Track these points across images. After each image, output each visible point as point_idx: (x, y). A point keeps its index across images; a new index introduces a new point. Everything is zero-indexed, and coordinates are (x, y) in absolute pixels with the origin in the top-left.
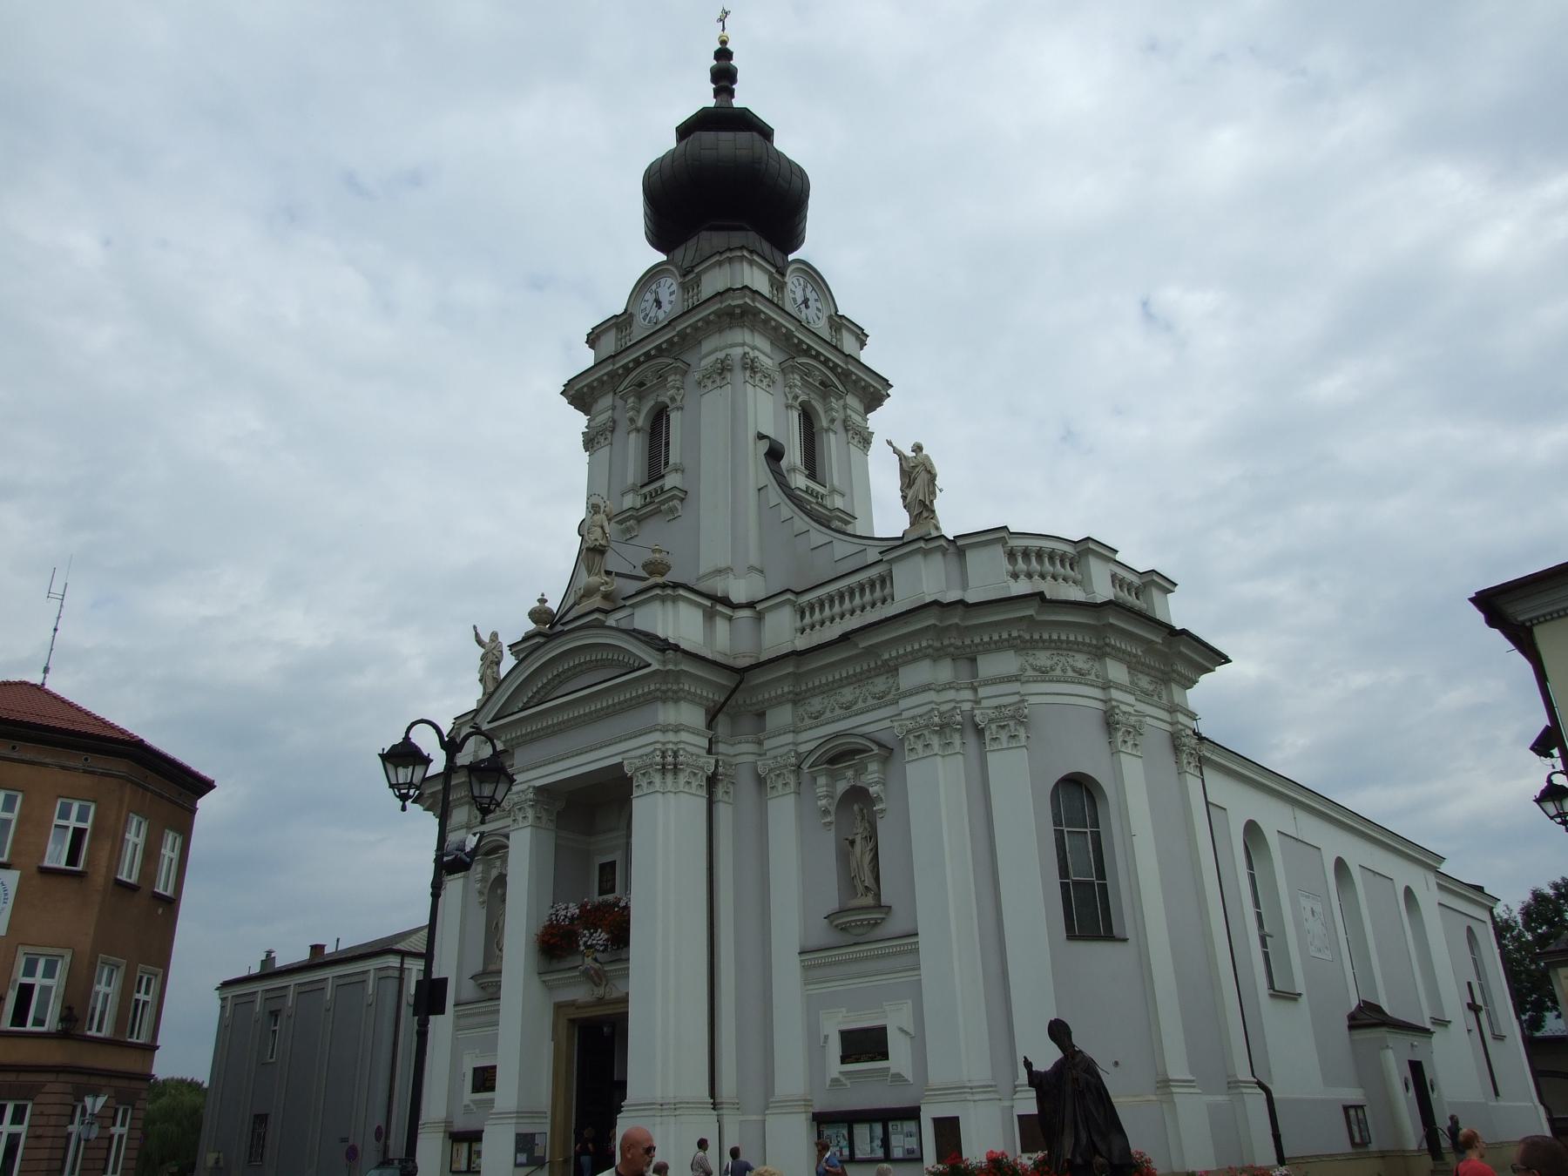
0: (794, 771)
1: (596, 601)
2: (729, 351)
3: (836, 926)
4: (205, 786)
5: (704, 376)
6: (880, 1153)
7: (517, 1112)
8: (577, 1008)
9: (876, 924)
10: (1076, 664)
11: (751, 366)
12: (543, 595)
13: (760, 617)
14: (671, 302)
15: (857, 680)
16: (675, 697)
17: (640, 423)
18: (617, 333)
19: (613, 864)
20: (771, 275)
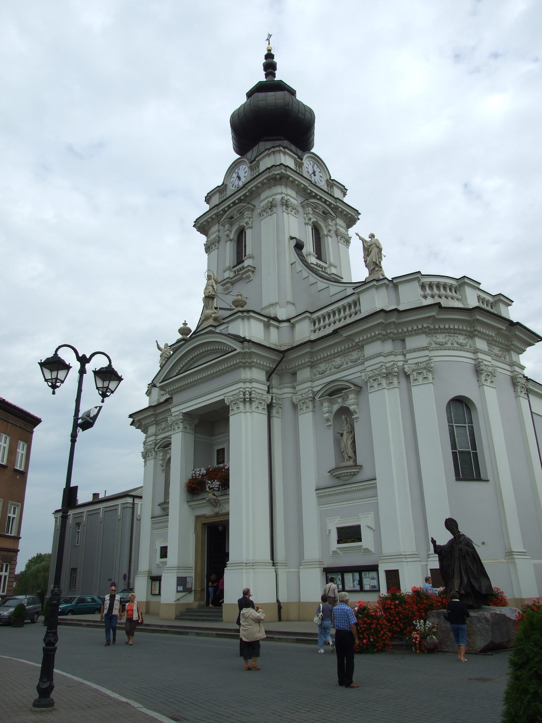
0: (311, 400)
1: (211, 322)
2: (274, 197)
3: (334, 476)
4: (36, 421)
5: (262, 211)
6: (358, 588)
7: (177, 567)
8: (206, 518)
10: (458, 341)
11: (286, 204)
12: (185, 321)
13: (293, 326)
14: (245, 177)
16: (250, 365)
17: (232, 236)
18: (219, 195)
19: (223, 450)
20: (295, 159)
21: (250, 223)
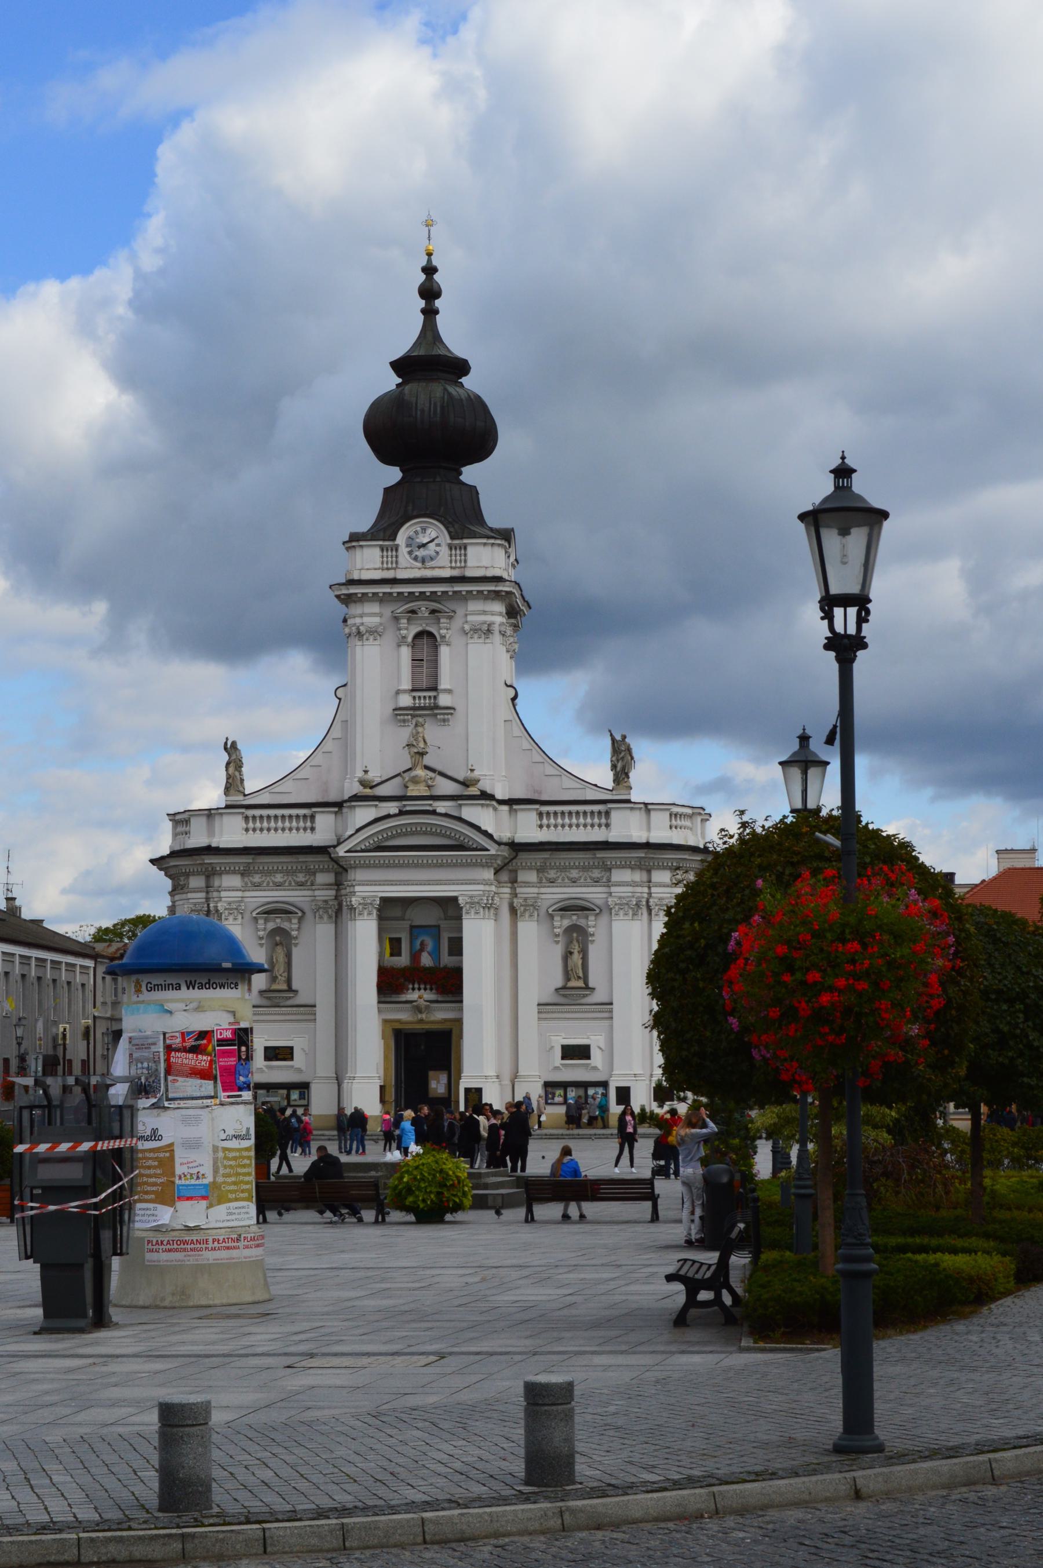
9: (585, 996)
15: (585, 869)
17: (410, 639)
21: (447, 636)
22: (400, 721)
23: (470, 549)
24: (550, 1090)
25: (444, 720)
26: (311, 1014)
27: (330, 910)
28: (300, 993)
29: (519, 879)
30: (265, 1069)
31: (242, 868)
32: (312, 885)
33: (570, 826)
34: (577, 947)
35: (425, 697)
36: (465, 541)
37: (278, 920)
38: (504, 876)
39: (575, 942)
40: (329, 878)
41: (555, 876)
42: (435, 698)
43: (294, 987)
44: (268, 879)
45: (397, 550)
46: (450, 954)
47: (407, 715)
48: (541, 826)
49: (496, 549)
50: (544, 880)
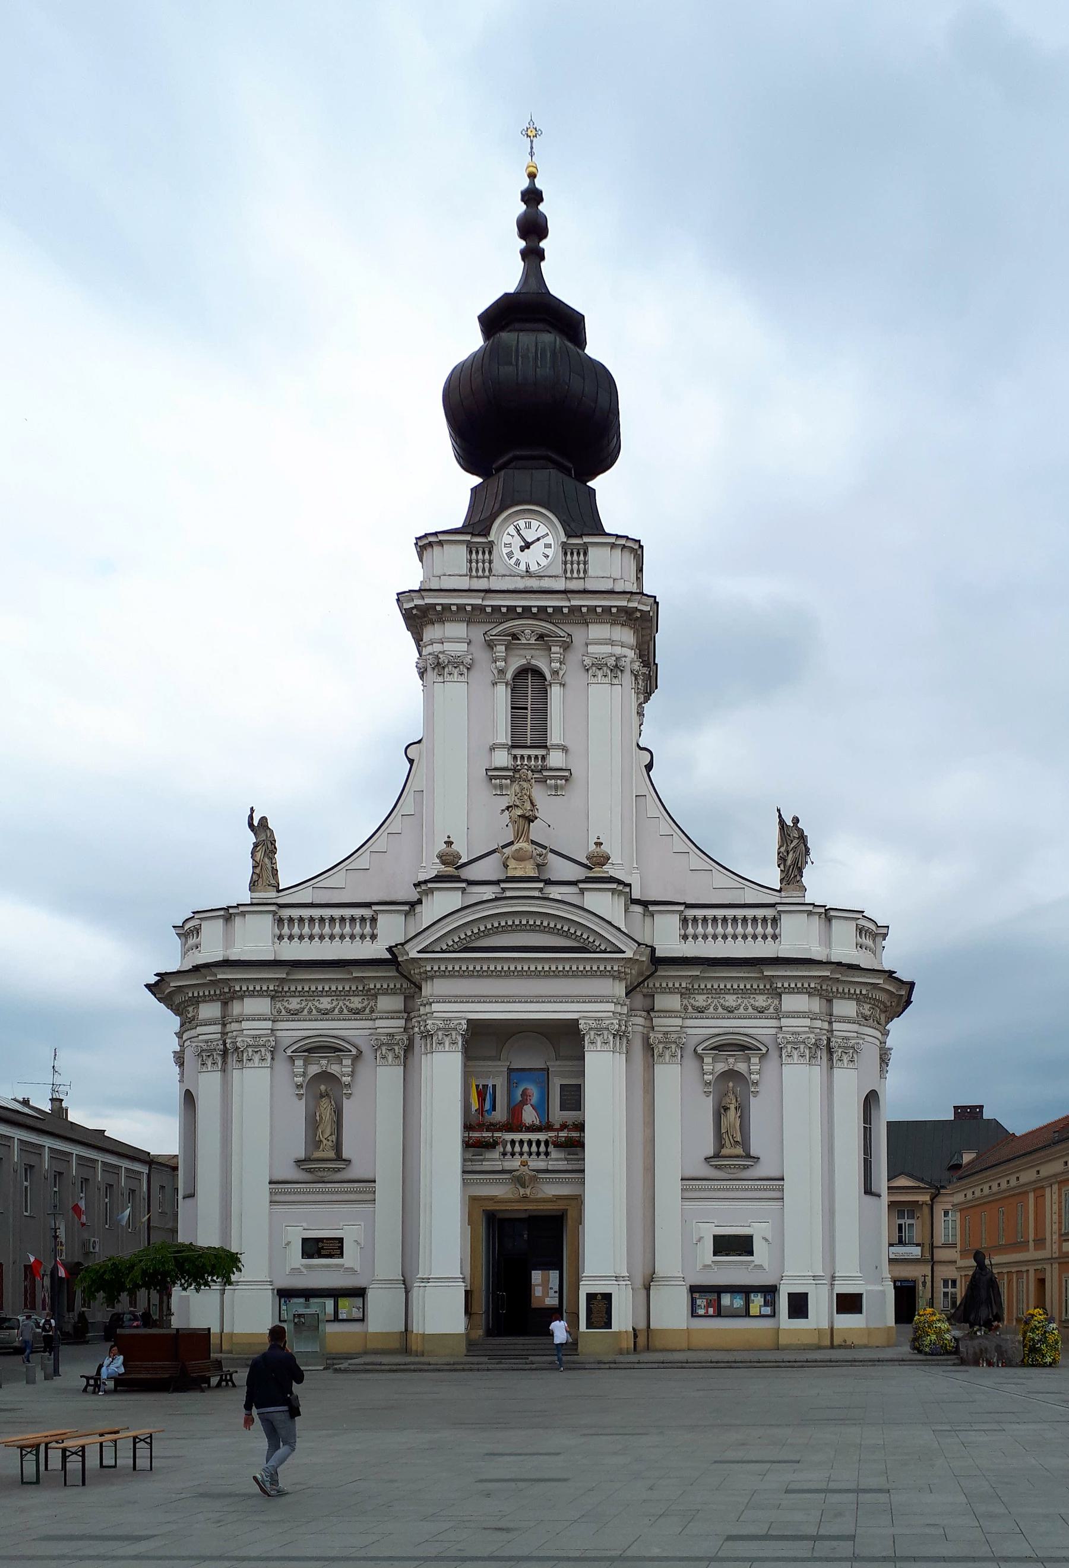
5: (593, 664)
15: (744, 993)
17: (509, 676)
21: (561, 673)
22: (495, 787)
23: (592, 552)
24: (696, 1295)
25: (556, 787)
26: (370, 1192)
27: (396, 1048)
28: (353, 1161)
29: (655, 1009)
30: (303, 1270)
31: (271, 988)
32: (372, 1011)
33: (725, 937)
34: (734, 1101)
35: (529, 757)
36: (586, 539)
37: (324, 1062)
38: (639, 1000)
39: (730, 1095)
40: (396, 1003)
41: (705, 1004)
42: (544, 758)
43: (344, 1156)
44: (310, 1004)
45: (490, 553)
46: (563, 1107)
47: (505, 777)
48: (685, 937)
49: (626, 554)
50: (690, 1009)
